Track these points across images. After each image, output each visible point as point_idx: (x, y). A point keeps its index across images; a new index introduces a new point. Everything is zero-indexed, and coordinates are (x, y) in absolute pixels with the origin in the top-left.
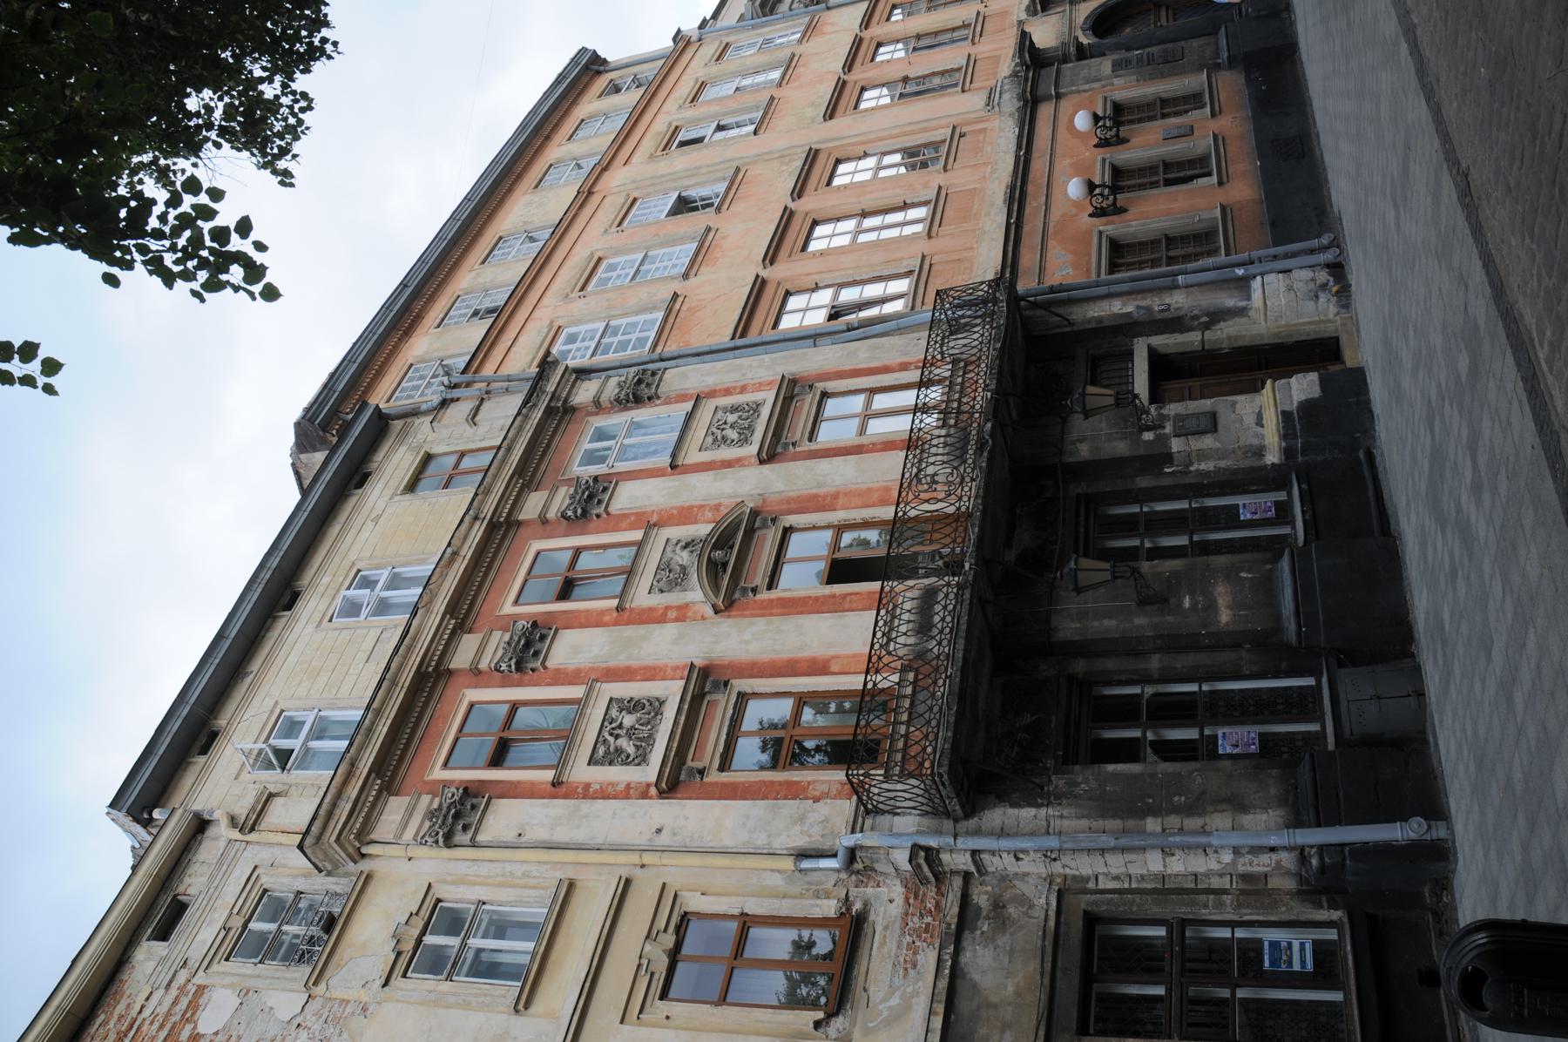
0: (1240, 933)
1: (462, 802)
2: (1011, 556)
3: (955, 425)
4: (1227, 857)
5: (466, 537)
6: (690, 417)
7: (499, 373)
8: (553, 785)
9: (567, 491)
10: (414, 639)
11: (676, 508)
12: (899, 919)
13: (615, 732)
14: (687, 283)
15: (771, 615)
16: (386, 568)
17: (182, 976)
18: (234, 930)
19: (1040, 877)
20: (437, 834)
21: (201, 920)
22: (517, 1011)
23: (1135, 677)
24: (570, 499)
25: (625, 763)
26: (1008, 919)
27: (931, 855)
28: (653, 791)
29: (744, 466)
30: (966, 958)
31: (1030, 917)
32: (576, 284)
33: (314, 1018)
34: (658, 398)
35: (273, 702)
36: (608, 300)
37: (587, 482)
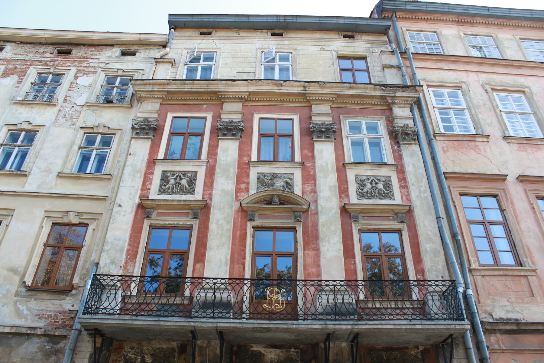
1: (150, 128)
5: (292, 86)
6: (384, 164)
10: (232, 85)
18: (116, 73)
20: (135, 124)
24: (322, 123)
32: (498, 86)
33: (74, 110)
34: (399, 147)
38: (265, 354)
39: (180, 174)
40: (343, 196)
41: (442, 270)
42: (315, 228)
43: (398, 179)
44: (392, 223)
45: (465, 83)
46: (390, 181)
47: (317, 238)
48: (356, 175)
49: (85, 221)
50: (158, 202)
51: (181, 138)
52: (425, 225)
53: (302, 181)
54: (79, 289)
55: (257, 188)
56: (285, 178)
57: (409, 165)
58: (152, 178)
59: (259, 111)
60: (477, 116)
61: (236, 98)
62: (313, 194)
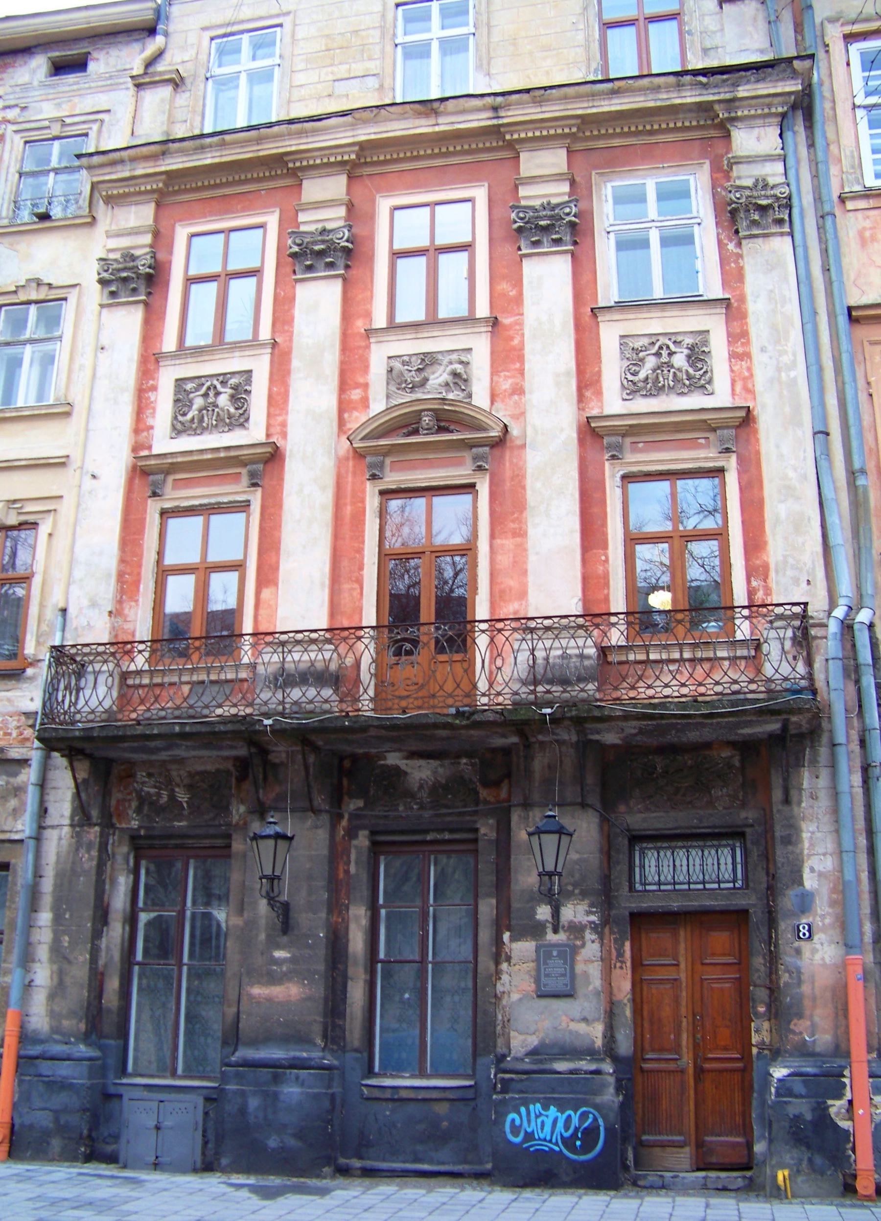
1: (139, 276)
2: (393, 759)
10: (314, 131)
11: (522, 343)
20: (106, 271)
24: (542, 205)
34: (739, 245)
38: (409, 770)
39: (215, 382)
40: (588, 394)
41: (809, 565)
42: (520, 482)
43: (729, 335)
44: (702, 453)
46: (706, 343)
47: (520, 506)
48: (622, 337)
49: (31, 518)
51: (213, 287)
52: (782, 456)
53: (492, 366)
55: (388, 397)
56: (451, 363)
57: (758, 297)
59: (389, 189)
61: (329, 165)
62: (516, 397)
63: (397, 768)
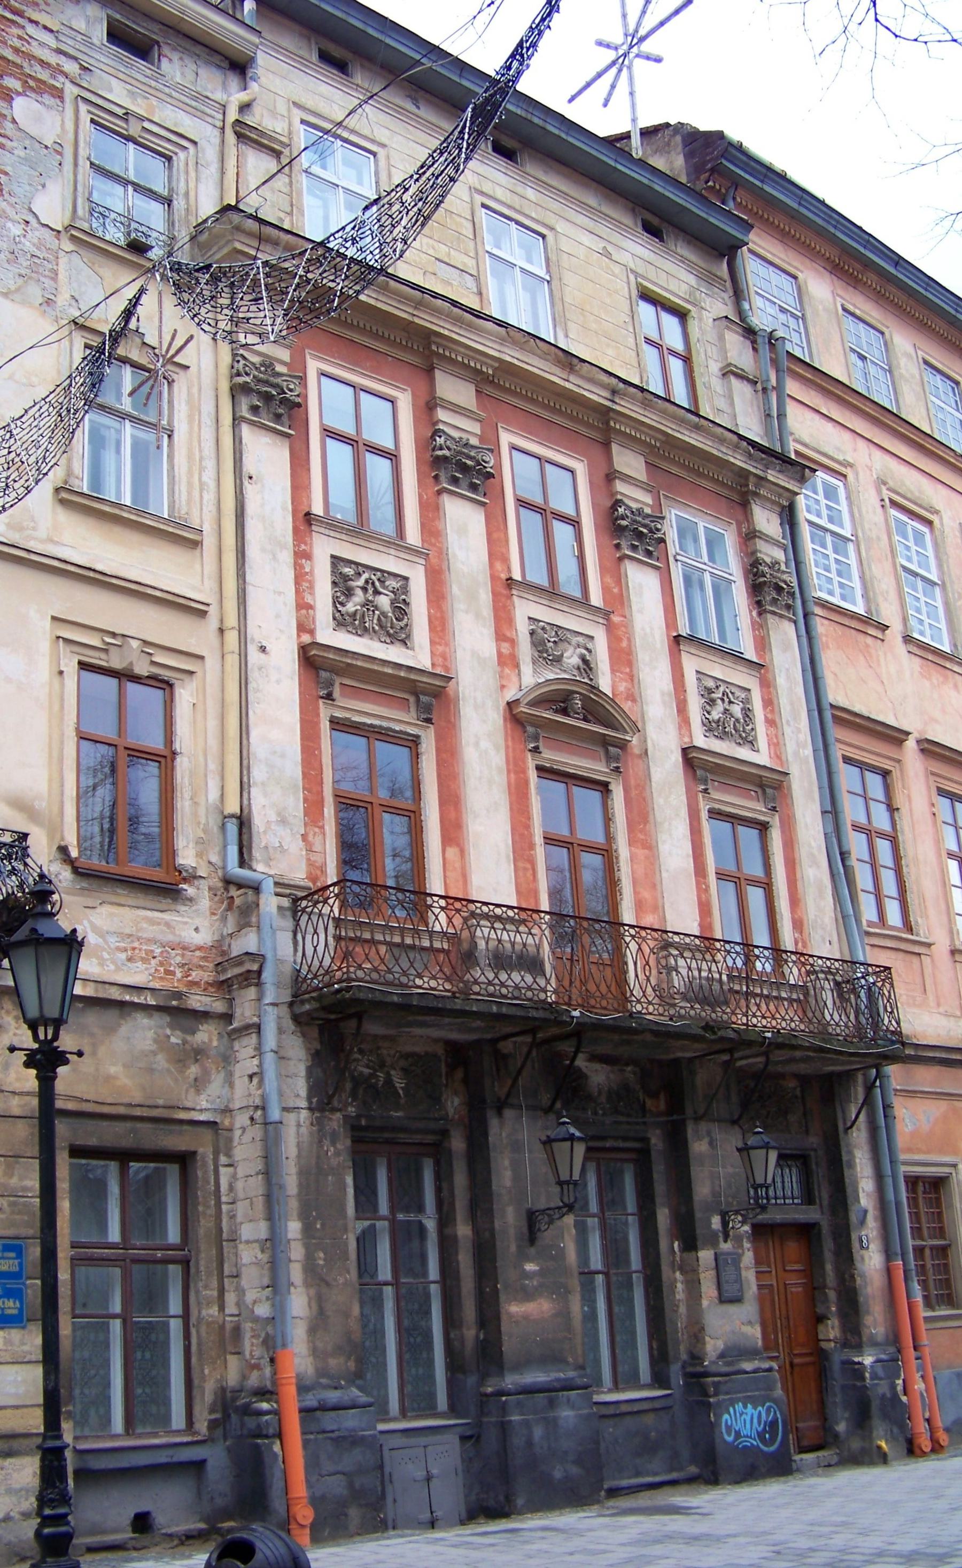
0: (175, 1326)
1: (285, 401)
3: (731, 990)
4: (263, 1310)
7: (788, 400)
8: (308, 514)
9: (648, 505)
10: (470, 326)
11: (629, 645)
12: (177, 940)
13: (370, 587)
14: (900, 639)
15: (509, 771)
16: (548, 271)
17: (71, 67)
18: (124, 125)
19: (229, 1101)
20: (247, 374)
21: (134, 82)
22: (57, 490)
23: (445, 1208)
24: (638, 510)
25: (336, 602)
26: (184, 1066)
27: (254, 978)
28: (306, 639)
29: (680, 728)
30: (143, 1020)
31: (187, 1091)
34: (760, 614)
35: (384, 140)
36: (879, 538)
37: (658, 530)
38: (589, 1073)
45: (851, 465)
50: (353, 658)
54: (196, 882)
56: (579, 646)
58: (312, 571)
60: (870, 568)
63: (579, 1070)
